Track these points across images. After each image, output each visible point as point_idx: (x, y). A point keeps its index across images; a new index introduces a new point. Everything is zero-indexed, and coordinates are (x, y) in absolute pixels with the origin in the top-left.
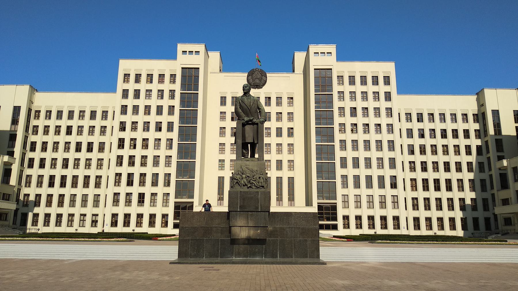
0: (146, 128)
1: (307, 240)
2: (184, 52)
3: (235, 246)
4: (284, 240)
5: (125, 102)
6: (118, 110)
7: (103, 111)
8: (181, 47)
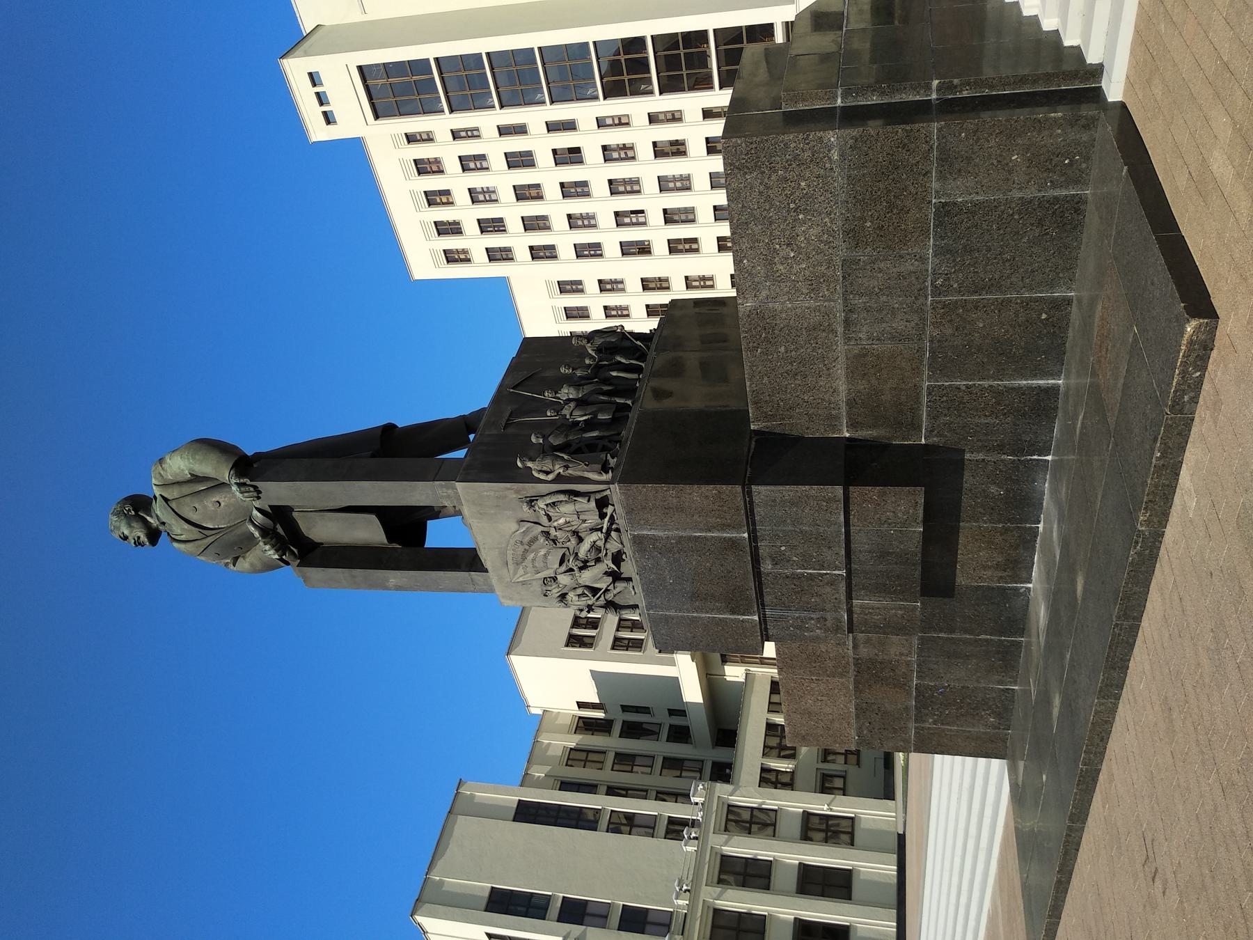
0: (579, 190)
1: (944, 205)
2: (328, 119)
3: (961, 580)
4: (932, 351)
5: (522, 254)
6: (545, 267)
7: (561, 292)
8: (318, 132)
